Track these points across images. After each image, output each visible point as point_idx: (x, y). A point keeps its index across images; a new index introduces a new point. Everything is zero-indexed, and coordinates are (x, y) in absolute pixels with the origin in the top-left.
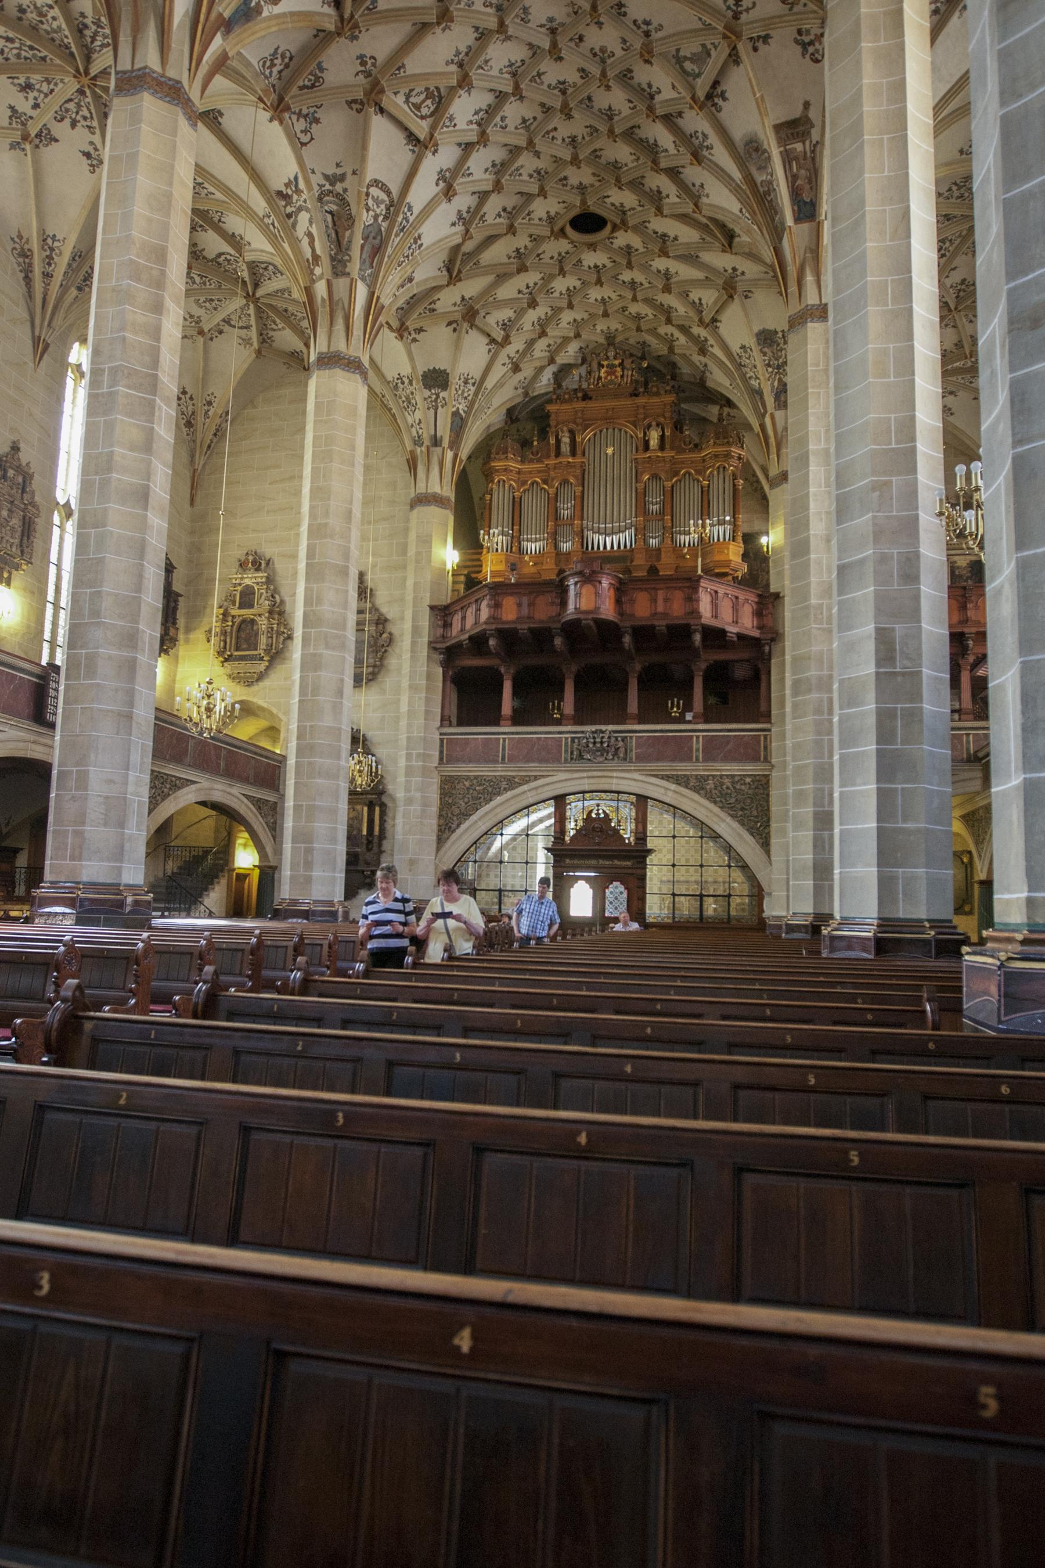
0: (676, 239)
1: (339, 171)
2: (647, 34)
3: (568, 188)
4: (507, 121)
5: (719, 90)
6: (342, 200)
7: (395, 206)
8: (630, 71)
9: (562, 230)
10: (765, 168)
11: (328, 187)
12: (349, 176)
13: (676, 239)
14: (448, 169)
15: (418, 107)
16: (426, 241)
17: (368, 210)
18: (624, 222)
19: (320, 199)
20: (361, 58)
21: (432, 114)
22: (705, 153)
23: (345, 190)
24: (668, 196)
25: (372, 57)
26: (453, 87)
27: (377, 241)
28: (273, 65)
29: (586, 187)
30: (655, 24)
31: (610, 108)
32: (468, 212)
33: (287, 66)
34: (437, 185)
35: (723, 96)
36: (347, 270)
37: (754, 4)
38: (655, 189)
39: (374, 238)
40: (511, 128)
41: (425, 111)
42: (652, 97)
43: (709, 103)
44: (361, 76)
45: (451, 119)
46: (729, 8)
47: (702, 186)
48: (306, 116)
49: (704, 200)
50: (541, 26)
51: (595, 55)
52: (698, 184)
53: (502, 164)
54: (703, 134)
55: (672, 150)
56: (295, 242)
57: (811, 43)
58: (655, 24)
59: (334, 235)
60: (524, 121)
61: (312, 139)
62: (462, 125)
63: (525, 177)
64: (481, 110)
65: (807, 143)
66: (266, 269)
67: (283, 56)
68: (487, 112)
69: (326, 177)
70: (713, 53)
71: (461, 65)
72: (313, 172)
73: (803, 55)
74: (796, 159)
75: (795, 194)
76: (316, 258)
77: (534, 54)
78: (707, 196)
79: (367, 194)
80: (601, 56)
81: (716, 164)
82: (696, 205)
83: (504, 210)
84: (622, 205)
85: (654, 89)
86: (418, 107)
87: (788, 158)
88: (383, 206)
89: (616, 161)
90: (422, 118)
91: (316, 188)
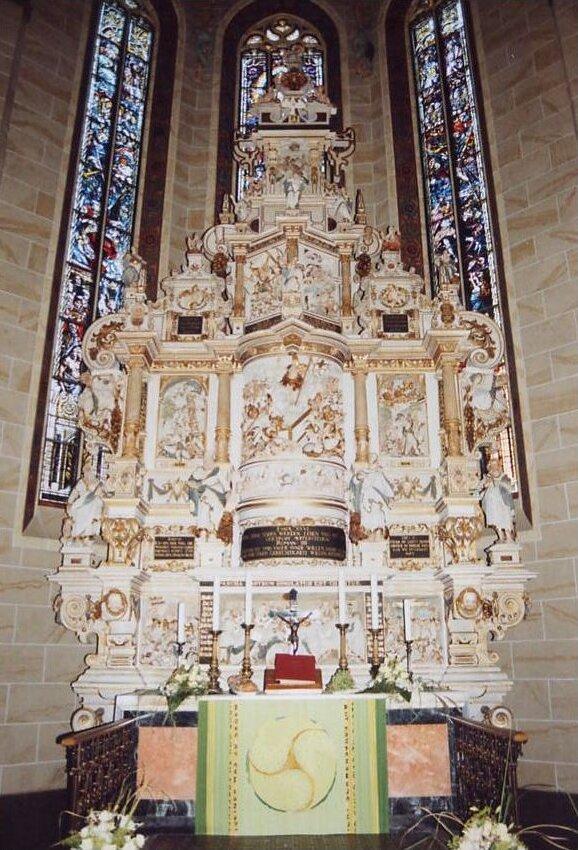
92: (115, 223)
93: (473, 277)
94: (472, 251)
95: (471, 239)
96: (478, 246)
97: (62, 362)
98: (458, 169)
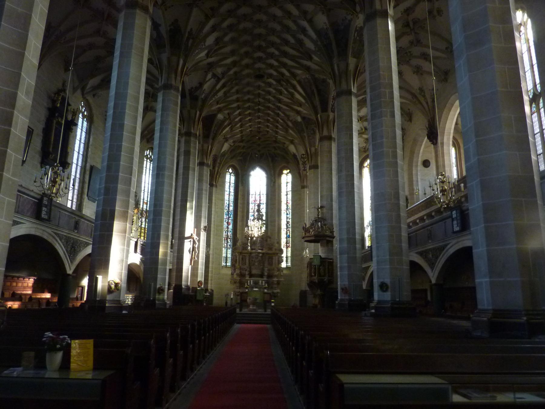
92: (230, 219)
93: (288, 232)
94: (288, 227)
95: (288, 225)
96: (289, 227)
97: (224, 245)
98: (287, 211)
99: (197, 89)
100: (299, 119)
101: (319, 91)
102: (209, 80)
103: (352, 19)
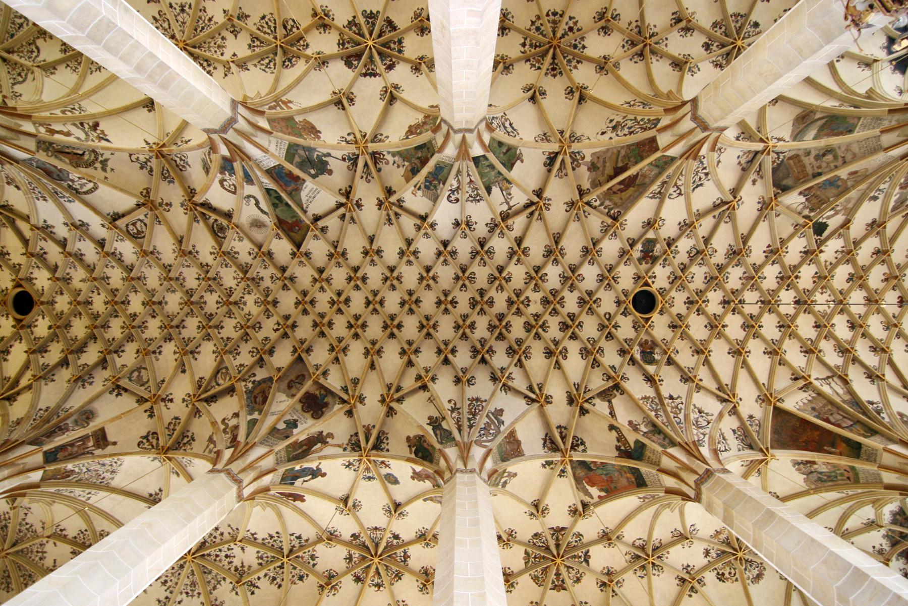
0: (5, 360)
1: (108, 169)
2: (154, 352)
3: (54, 295)
4: (110, 269)
5: (122, 392)
6: (89, 165)
7: (77, 193)
8: (132, 341)
9: (19, 286)
10: (77, 425)
11: (100, 159)
12: (103, 174)
13: (5, 360)
14: (88, 229)
15: (134, 224)
16: (40, 204)
17: (79, 178)
18: (22, 327)
19: (94, 151)
20: (170, 205)
21: (128, 231)
22: (80, 384)
23: (96, 168)
24: (43, 357)
25: (169, 210)
26: (142, 247)
27: (55, 176)
28: (181, 159)
29: (53, 305)
30: (160, 357)
31: (110, 327)
32: (51, 232)
33: (177, 166)
34: (80, 221)
35: (119, 394)
36: (41, 151)
37: (168, 409)
38: (49, 349)
39: (58, 175)
40: (106, 270)
41: (131, 227)
42: (116, 352)
43: (114, 387)
44: (160, 201)
45: (122, 240)
46: (167, 396)
47: (53, 380)
48: (146, 163)
49: (43, 382)
50: (164, 298)
51: (143, 323)
52: (55, 378)
53: (81, 260)
54: (92, 382)
55: (80, 362)
56: (64, 122)
57: (148, 440)
58: (160, 357)
59: (67, 150)
60: (108, 278)
61: (132, 161)
62: (116, 244)
63: (68, 270)
64: (122, 256)
65: (93, 448)
66: (19, 74)
67: (184, 167)
68: (119, 259)
69: (106, 160)
70: (143, 388)
71: (152, 253)
72: (112, 154)
73: (142, 437)
74: (84, 444)
75: (62, 448)
76: (53, 132)
77: (149, 291)
78: (46, 384)
79: (90, 181)
80: (143, 326)
81: (73, 391)
82: (40, 377)
83: (45, 253)
84: (36, 326)
85: (121, 354)
86: (134, 224)
87: (85, 438)
88: (78, 187)
89: (71, 326)
90: (127, 225)
91: (102, 152)
99: (621, 438)
100: (794, 199)
101: (618, 171)
102: (611, 407)
103: (389, 153)
